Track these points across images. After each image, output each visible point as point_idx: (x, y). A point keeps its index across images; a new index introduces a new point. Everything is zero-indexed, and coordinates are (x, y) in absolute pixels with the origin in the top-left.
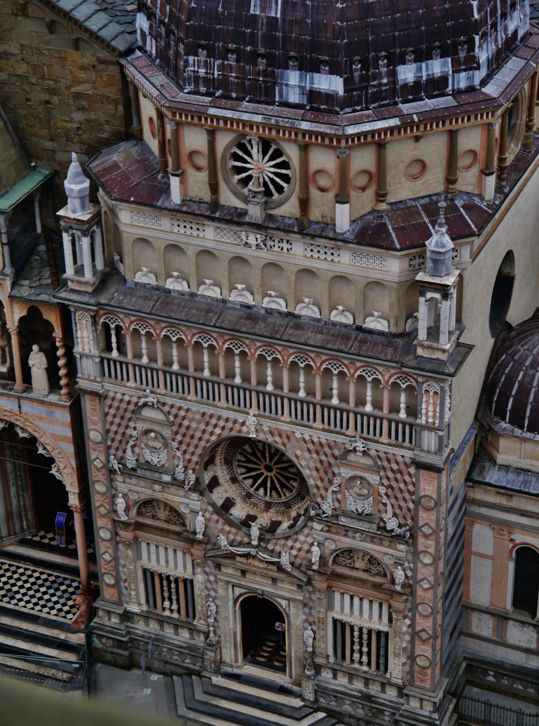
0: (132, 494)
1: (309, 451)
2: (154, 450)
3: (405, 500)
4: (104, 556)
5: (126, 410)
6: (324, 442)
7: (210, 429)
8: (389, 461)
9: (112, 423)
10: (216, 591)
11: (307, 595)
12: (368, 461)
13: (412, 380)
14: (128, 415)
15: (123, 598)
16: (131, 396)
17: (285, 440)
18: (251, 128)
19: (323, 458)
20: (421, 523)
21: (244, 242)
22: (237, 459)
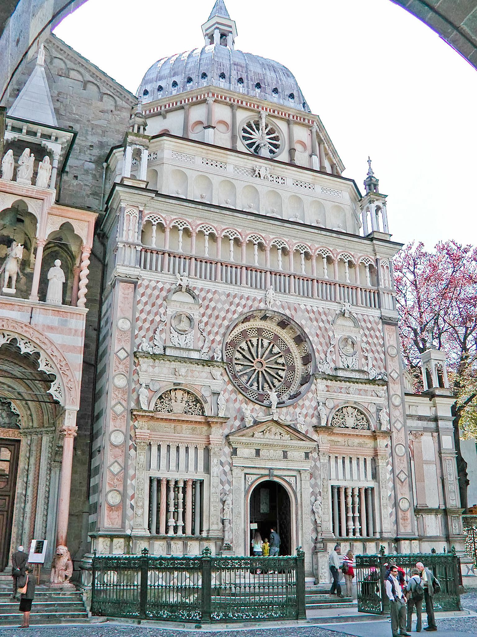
0: (153, 385)
1: (311, 319)
2: (182, 332)
3: (378, 352)
4: (112, 469)
5: (158, 297)
6: (321, 310)
7: (233, 308)
8: (365, 321)
9: (142, 311)
10: (230, 483)
11: (313, 463)
12: (351, 324)
13: (371, 260)
14: (159, 302)
15: (127, 522)
16: (164, 283)
17: (293, 312)
18: (263, 109)
19: (321, 324)
20: (390, 371)
21: (257, 173)
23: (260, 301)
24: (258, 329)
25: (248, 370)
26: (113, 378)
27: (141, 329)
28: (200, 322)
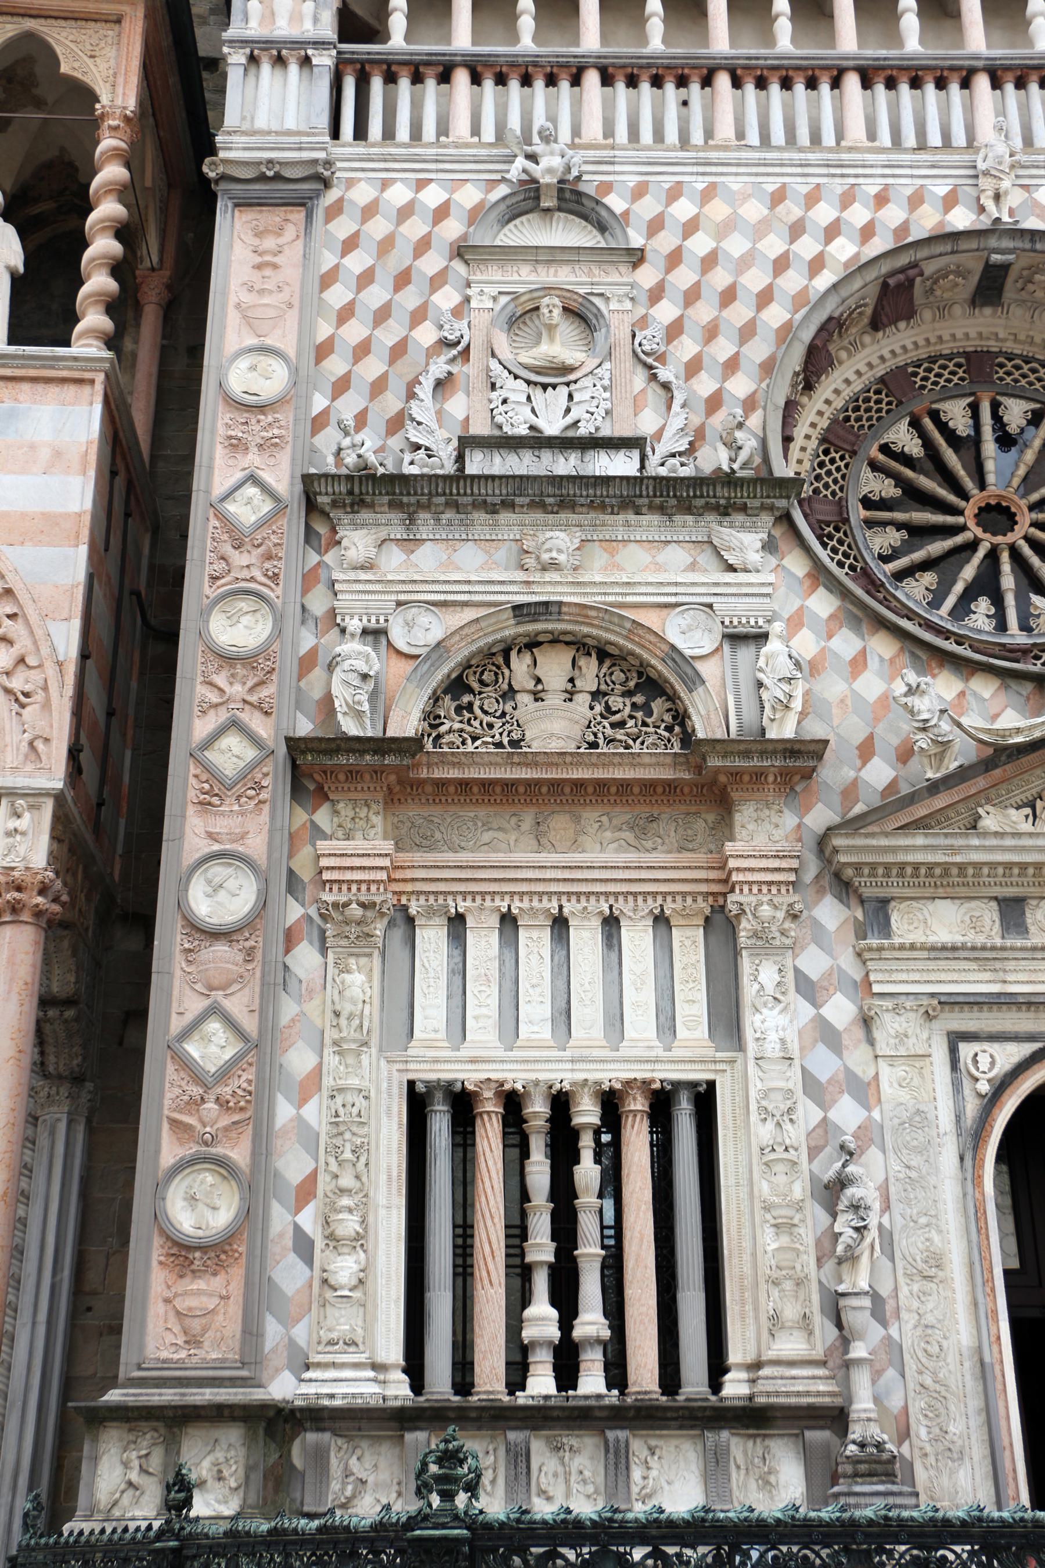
0: (409, 625)
4: (193, 1049)
5: (423, 246)
7: (807, 247)
9: (346, 314)
14: (432, 263)
15: (273, 1330)
22: (865, 490)
23: (950, 202)
24: (966, 355)
25: (938, 547)
26: (205, 614)
27: (341, 386)
28: (643, 322)
